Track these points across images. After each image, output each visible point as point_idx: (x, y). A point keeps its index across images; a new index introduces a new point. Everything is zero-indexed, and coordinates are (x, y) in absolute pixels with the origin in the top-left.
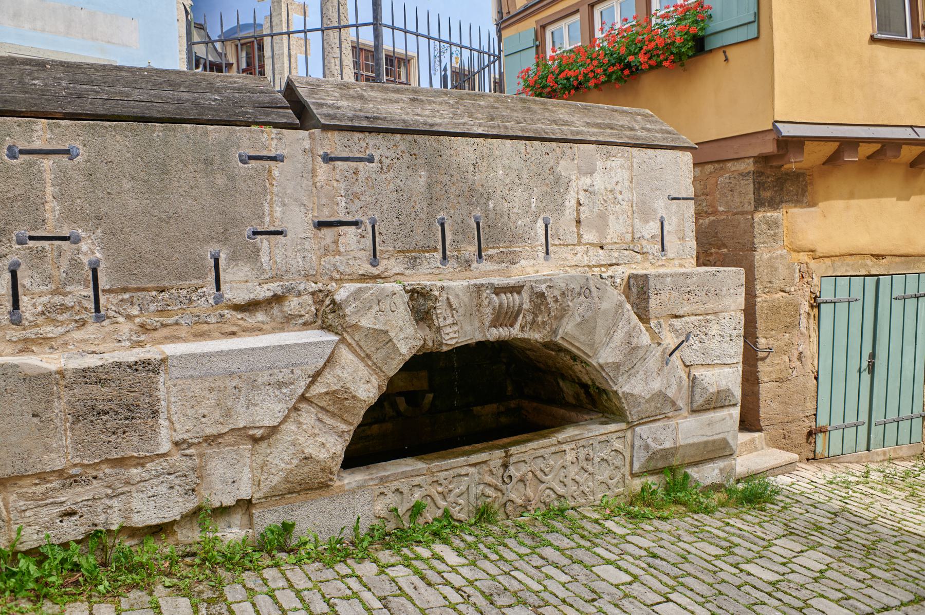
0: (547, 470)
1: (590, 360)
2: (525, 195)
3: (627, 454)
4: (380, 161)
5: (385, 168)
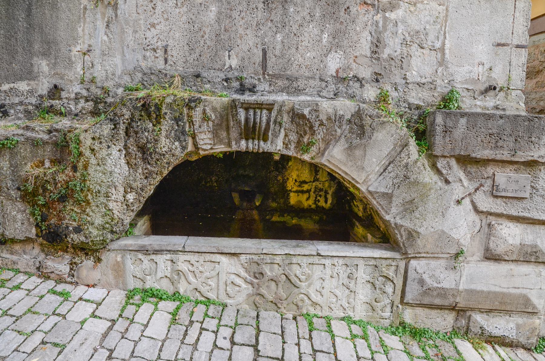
0: (303, 278)
1: (358, 185)
2: (316, 31)
5: (179, 4)
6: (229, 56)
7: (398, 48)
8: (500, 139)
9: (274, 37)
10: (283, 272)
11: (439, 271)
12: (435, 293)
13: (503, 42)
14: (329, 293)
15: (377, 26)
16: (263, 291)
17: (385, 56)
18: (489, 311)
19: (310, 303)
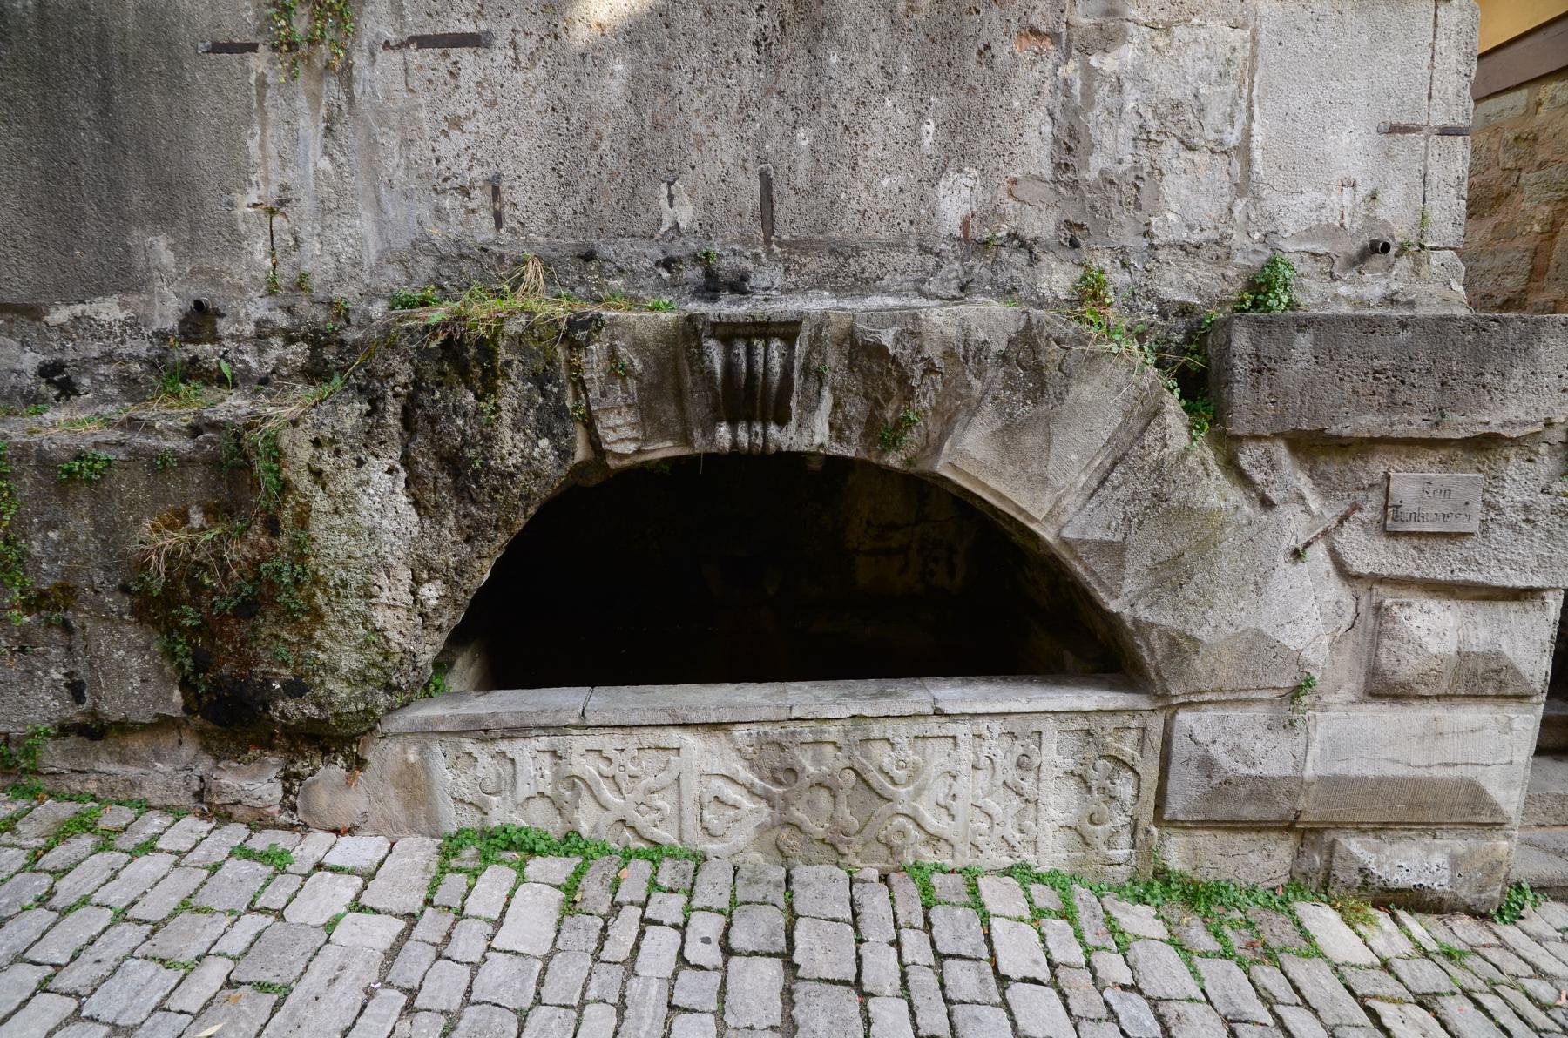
0: (900, 774)
1: (1034, 527)
2: (903, 116)
3: (1150, 771)
4: (514, 45)
5: (522, 58)
6: (671, 197)
7: (1126, 152)
8: (1403, 382)
9: (789, 137)
10: (848, 763)
11: (1251, 734)
12: (1243, 791)
13: (1405, 120)
14: (970, 809)
15: (1067, 94)
16: (798, 814)
17: (1092, 175)
18: (1381, 828)
19: (922, 836)
